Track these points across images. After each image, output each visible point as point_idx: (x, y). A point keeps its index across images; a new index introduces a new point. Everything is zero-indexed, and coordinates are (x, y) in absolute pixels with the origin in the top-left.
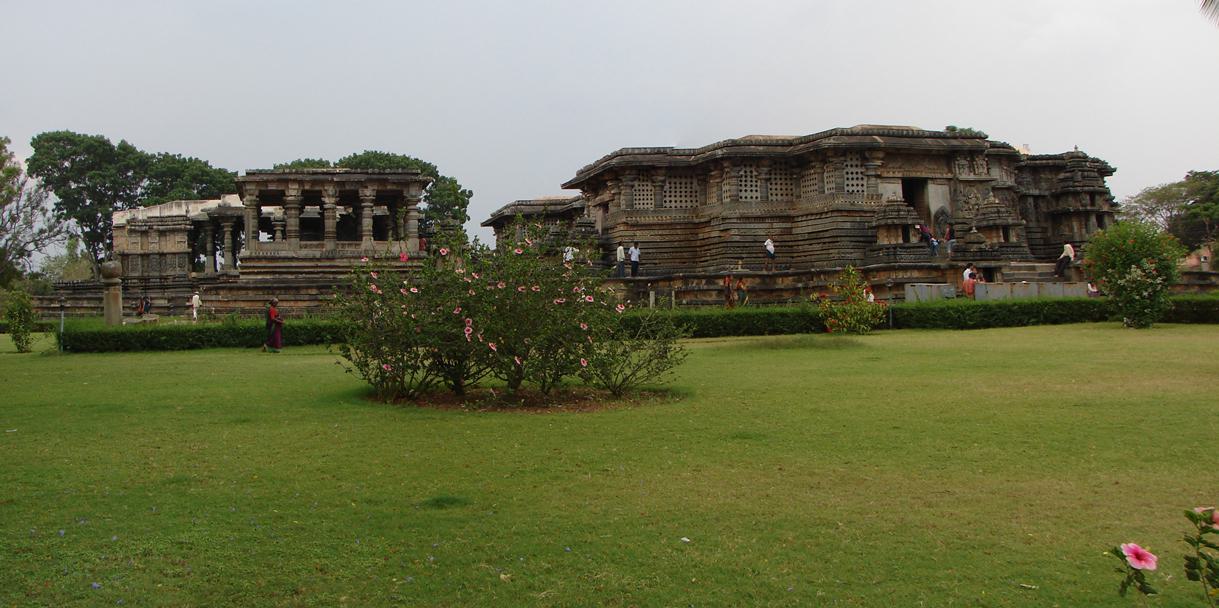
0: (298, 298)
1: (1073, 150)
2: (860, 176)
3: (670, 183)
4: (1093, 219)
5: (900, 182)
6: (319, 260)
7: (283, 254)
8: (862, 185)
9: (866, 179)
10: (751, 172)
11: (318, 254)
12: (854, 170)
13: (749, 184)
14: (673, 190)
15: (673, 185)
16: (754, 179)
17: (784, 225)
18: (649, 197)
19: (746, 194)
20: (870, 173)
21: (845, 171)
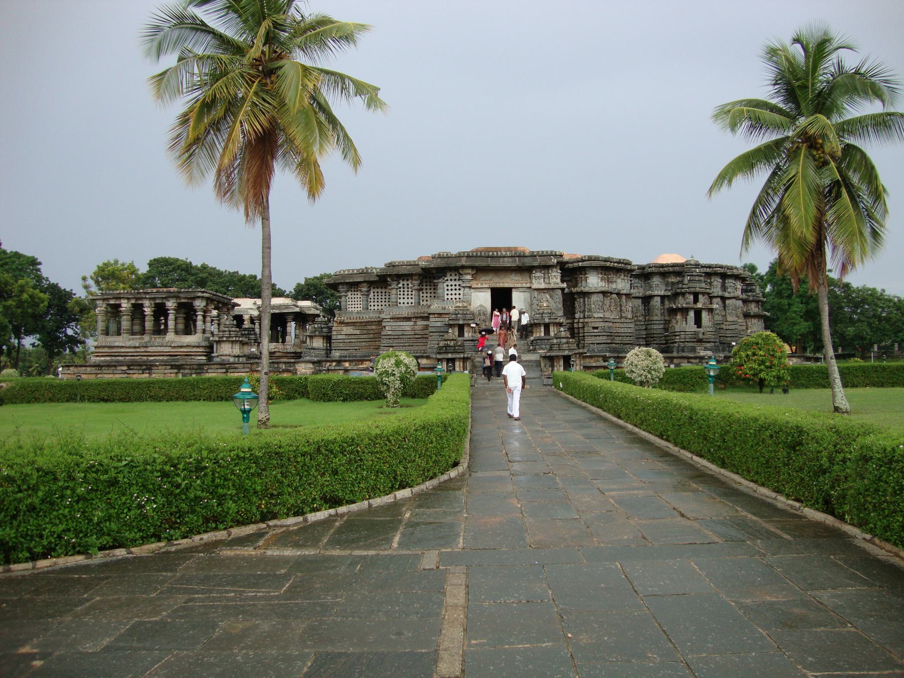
0: (115, 372)
2: (457, 287)
4: (692, 314)
5: (489, 291)
7: (117, 344)
9: (462, 289)
10: (408, 285)
12: (453, 283)
13: (406, 293)
14: (376, 297)
15: (376, 294)
16: (410, 290)
17: (425, 323)
18: (359, 303)
19: (404, 301)
20: (464, 285)
21: (445, 285)
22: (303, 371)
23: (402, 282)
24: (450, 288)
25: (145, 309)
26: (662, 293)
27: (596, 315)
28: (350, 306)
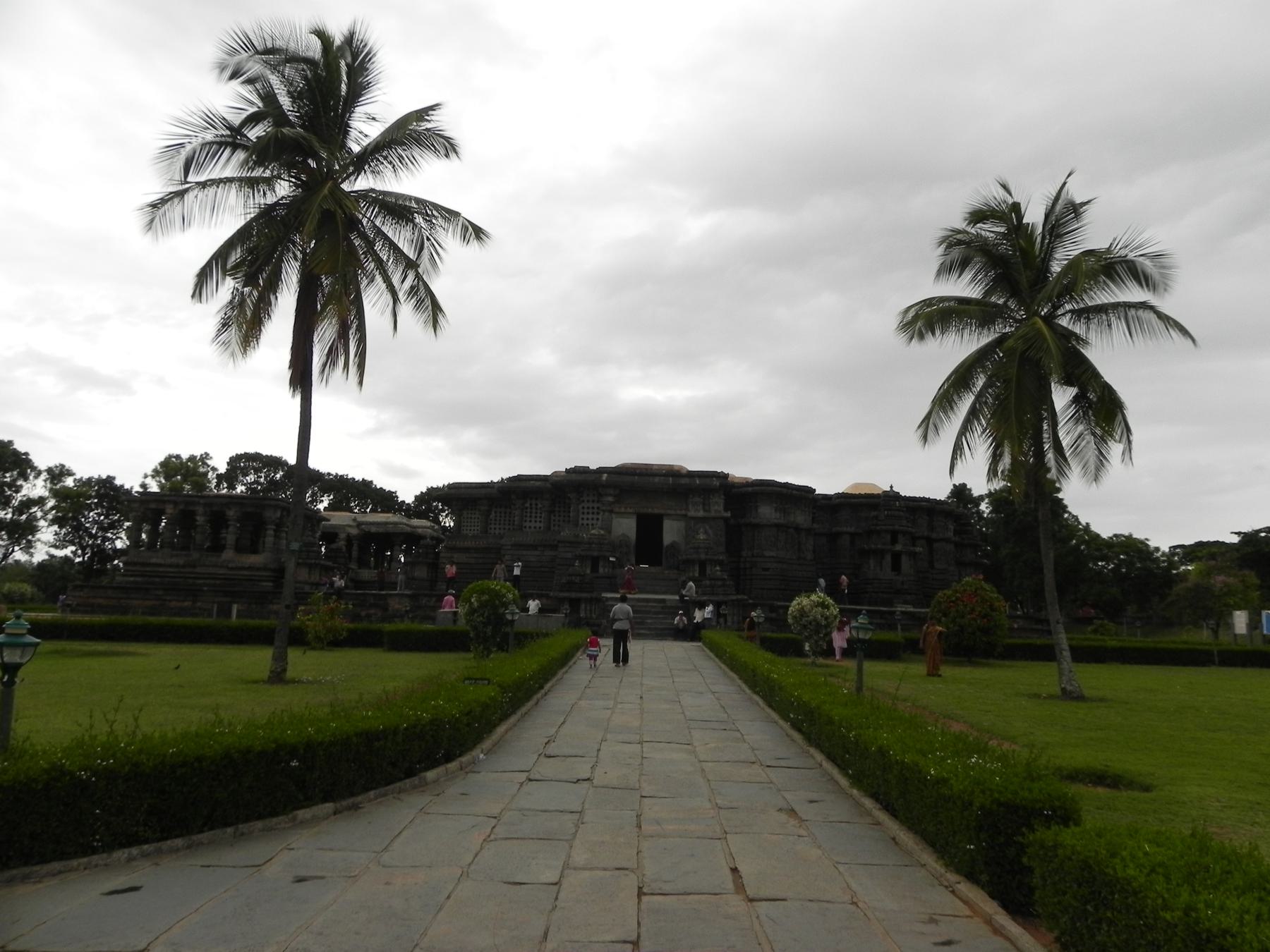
1: (889, 489)
2: (596, 510)
3: (496, 512)
4: (888, 558)
5: (635, 517)
6: (183, 566)
7: (154, 560)
8: (598, 519)
9: (602, 513)
10: (536, 505)
11: (181, 562)
12: (591, 505)
13: (534, 515)
14: (498, 518)
15: (498, 515)
16: (539, 511)
20: (604, 508)
21: (580, 507)
22: (397, 606)
23: (529, 502)
24: (586, 511)
25: (198, 518)
26: (852, 530)
27: (767, 553)
28: (465, 528)
